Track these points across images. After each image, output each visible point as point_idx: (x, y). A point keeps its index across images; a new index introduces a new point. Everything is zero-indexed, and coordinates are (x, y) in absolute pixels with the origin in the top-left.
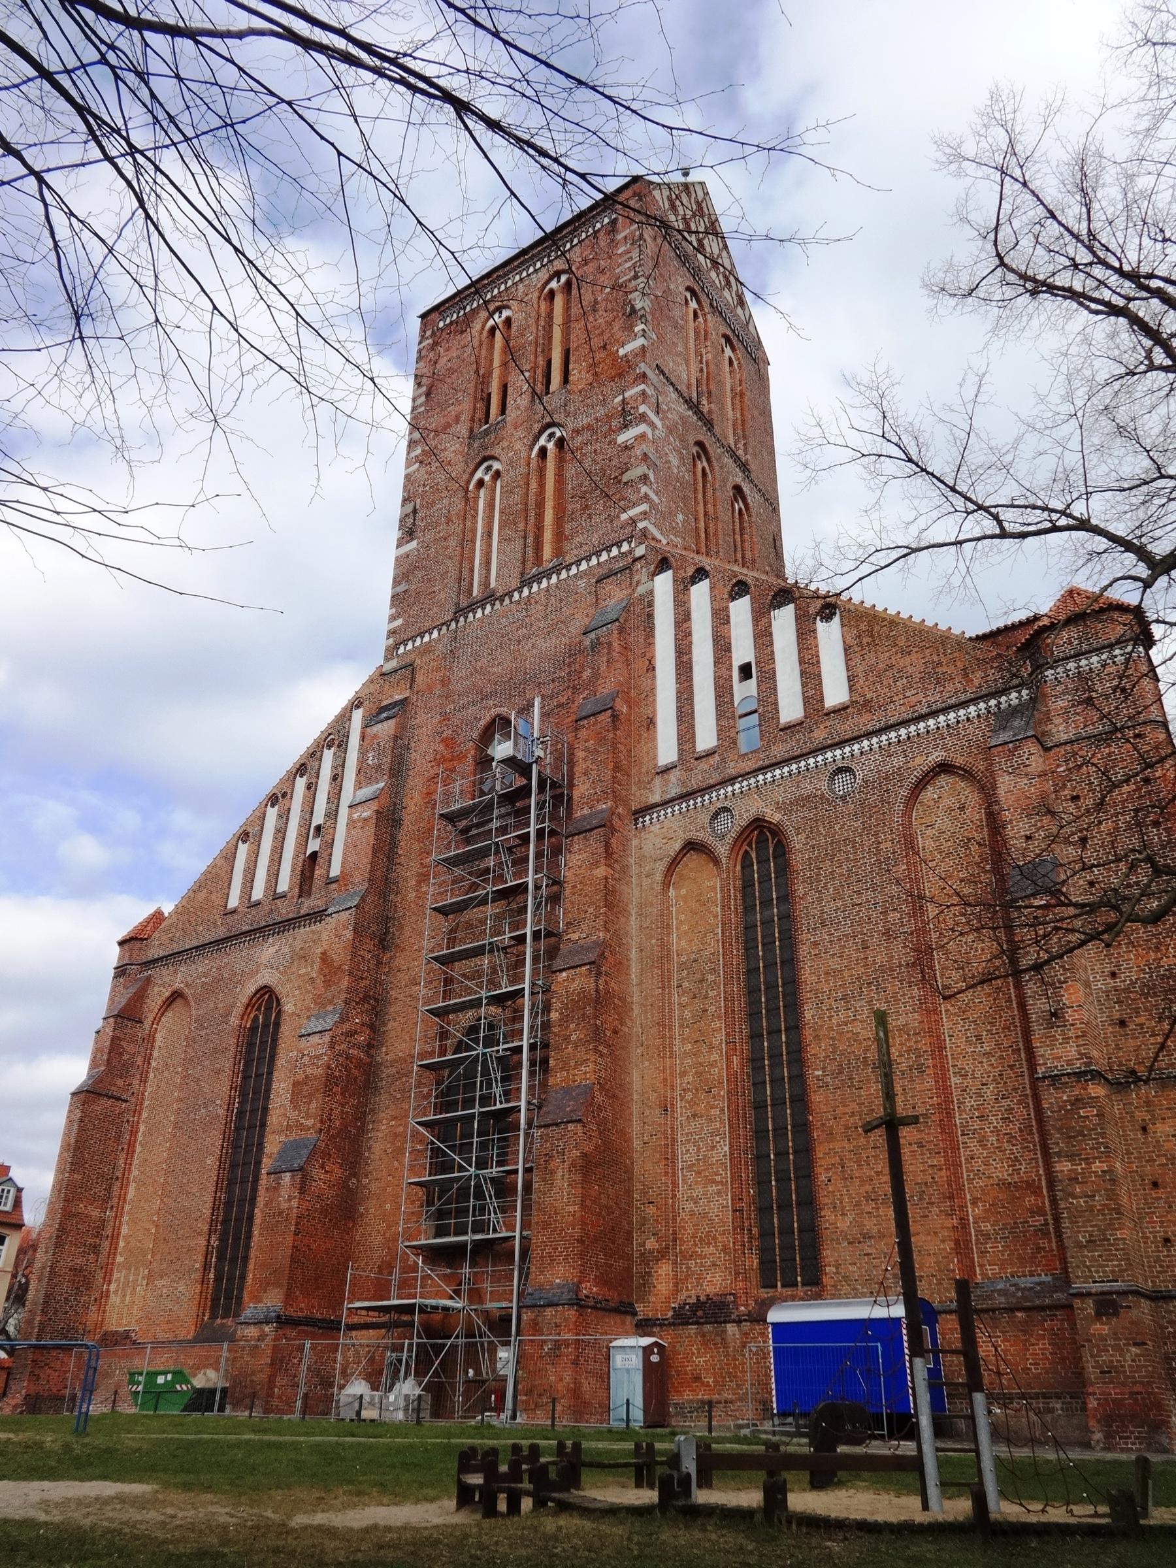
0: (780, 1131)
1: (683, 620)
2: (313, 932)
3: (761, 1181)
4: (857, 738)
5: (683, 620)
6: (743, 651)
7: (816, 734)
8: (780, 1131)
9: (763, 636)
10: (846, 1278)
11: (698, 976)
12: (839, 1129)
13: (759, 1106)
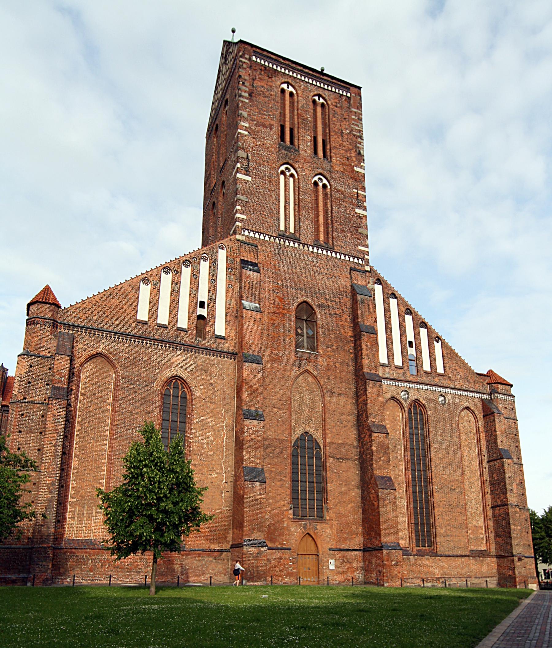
0: (421, 501)
1: (387, 311)
2: (210, 360)
3: (416, 513)
4: (447, 388)
5: (387, 311)
6: (410, 337)
7: (435, 380)
8: (421, 501)
9: (417, 335)
10: (443, 546)
11: (394, 445)
12: (441, 505)
13: (414, 492)
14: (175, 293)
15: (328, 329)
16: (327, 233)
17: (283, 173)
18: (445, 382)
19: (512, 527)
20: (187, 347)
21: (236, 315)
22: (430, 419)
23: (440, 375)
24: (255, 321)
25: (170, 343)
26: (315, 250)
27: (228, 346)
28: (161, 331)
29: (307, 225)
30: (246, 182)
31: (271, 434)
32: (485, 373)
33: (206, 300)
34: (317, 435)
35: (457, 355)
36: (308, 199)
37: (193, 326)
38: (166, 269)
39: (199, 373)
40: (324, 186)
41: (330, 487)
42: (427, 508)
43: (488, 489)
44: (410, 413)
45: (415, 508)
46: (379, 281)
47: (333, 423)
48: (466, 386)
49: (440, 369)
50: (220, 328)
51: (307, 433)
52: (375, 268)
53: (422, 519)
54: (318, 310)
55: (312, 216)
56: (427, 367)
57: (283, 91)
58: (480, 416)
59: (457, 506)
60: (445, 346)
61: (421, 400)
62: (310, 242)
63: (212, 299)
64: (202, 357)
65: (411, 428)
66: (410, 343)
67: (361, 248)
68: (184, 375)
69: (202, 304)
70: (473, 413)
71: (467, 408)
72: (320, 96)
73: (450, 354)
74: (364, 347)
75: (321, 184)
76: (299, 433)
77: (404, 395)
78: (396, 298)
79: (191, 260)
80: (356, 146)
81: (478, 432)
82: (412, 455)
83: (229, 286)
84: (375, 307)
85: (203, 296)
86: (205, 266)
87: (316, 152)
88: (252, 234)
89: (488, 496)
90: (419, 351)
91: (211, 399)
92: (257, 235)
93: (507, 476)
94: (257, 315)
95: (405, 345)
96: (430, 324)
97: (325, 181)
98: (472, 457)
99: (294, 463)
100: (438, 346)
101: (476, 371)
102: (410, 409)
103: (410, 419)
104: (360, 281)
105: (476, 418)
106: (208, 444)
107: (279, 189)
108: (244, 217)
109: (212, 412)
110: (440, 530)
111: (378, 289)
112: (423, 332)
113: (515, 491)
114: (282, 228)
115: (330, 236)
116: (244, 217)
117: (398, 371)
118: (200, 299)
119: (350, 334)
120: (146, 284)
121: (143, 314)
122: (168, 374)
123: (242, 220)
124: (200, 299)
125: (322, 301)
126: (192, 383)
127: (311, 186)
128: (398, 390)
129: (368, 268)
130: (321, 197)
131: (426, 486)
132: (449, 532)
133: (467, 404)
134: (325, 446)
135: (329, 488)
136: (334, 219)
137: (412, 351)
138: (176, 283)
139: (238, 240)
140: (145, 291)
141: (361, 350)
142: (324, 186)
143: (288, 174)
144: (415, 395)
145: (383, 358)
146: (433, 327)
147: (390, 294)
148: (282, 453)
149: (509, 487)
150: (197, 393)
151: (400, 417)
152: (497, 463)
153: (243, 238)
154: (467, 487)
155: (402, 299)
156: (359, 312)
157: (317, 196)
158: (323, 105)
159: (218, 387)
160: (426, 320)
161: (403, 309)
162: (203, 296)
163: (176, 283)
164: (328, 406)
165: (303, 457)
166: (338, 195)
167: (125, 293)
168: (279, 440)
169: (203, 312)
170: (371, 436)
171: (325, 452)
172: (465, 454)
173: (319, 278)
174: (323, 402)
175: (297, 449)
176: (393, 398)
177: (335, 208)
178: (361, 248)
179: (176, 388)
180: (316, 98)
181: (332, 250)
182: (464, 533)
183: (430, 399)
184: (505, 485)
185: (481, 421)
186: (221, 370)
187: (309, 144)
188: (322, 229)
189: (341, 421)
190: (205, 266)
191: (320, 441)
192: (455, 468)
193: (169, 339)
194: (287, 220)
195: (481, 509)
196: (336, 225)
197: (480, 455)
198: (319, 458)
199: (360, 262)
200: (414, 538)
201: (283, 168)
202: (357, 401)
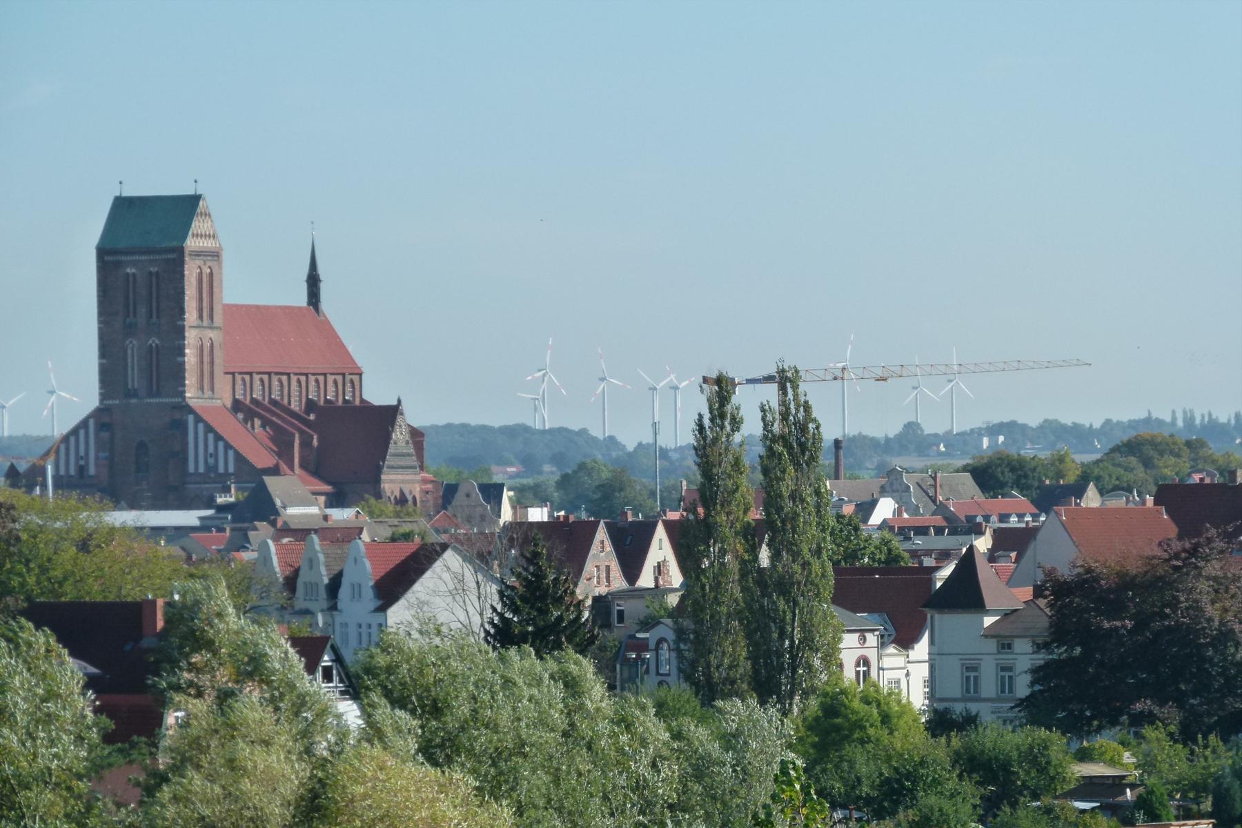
1: (196, 433)
5: (196, 433)
6: (211, 449)
9: (216, 448)
14: (67, 454)
56: (221, 470)
85: (82, 453)
100: (231, 453)
104: (177, 416)
111: (191, 418)
145: (191, 469)
147: (199, 420)
162: (82, 453)
181: (158, 395)
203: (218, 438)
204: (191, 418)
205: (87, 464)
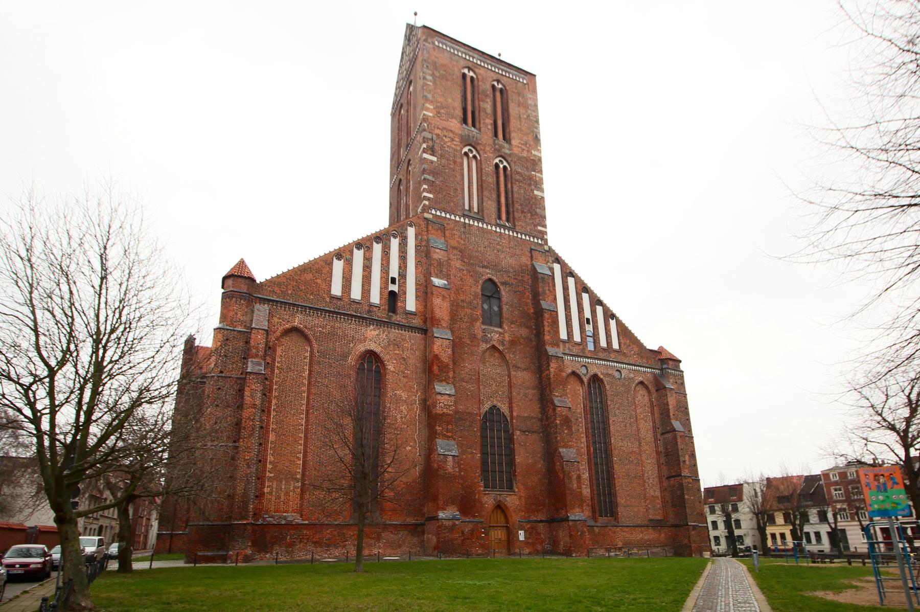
1: (566, 289)
2: (401, 335)
5: (566, 289)
6: (588, 314)
9: (594, 312)
13: (596, 464)
14: (367, 268)
15: (511, 306)
16: (508, 213)
17: (466, 154)
18: (619, 358)
19: (686, 497)
20: (380, 323)
21: (425, 291)
22: (608, 393)
23: (616, 351)
24: (444, 297)
25: (363, 318)
26: (498, 230)
27: (416, 322)
28: (354, 306)
29: (490, 206)
30: (432, 162)
31: (461, 408)
32: (656, 348)
33: (396, 276)
34: (505, 409)
35: (630, 332)
36: (491, 179)
37: (385, 301)
38: (359, 245)
39: (391, 348)
40: (505, 168)
41: (518, 459)
42: (608, 479)
43: (662, 460)
44: (589, 387)
45: (597, 479)
46: (558, 260)
47: (518, 397)
48: (639, 362)
49: (616, 346)
50: (411, 304)
51: (495, 406)
52: (553, 248)
53: (604, 490)
54: (502, 288)
55: (494, 196)
56: (603, 343)
57: (464, 75)
58: (653, 390)
59: (635, 477)
60: (620, 324)
61: (599, 374)
62: (493, 222)
63: (403, 275)
64: (395, 333)
65: (591, 401)
66: (588, 320)
67: (540, 228)
68: (378, 350)
69: (393, 281)
70: (647, 387)
71: (641, 383)
72: (498, 81)
73: (624, 331)
74: (546, 323)
75: (501, 166)
76: (486, 407)
77: (584, 370)
78: (573, 276)
79: (381, 237)
80: (533, 132)
81: (652, 406)
82: (593, 428)
83: (418, 263)
84: (554, 285)
85: (394, 272)
86: (395, 243)
87: (496, 135)
88: (438, 213)
89: (664, 468)
90: (595, 328)
91: (404, 373)
92: (443, 215)
93: (680, 447)
94: (444, 293)
95: (583, 322)
96: (605, 302)
97: (505, 164)
98: (646, 428)
99: (483, 437)
100: (613, 323)
101: (648, 347)
102: (589, 383)
103: (590, 393)
105: (649, 392)
106: (401, 418)
107: (463, 169)
108: (431, 196)
109: (405, 386)
110: (621, 500)
111: (557, 267)
112: (599, 309)
113: (687, 463)
114: (467, 207)
115: (511, 216)
116: (431, 196)
117: (577, 347)
118: (391, 275)
119: (532, 311)
120: (339, 259)
121: (336, 289)
122: (361, 348)
123: (428, 199)
124: (391, 275)
125: (506, 278)
126: (385, 357)
127: (492, 168)
128: (578, 365)
129: (546, 248)
130: (502, 179)
131: (606, 458)
132: (628, 503)
133: (641, 379)
134: (512, 418)
135: (518, 460)
136: (515, 200)
137: (589, 328)
138: (368, 260)
139: (426, 219)
140: (338, 266)
141: (543, 326)
142: (505, 168)
143: (471, 155)
144: (593, 370)
145: (563, 335)
146: (608, 305)
147: (568, 272)
148: (471, 426)
149: (682, 459)
150: (390, 367)
151: (581, 391)
152: (669, 436)
153: (430, 216)
154: (643, 458)
155: (579, 278)
156: (541, 290)
157: (498, 178)
158: (501, 90)
159: (411, 362)
160: (602, 299)
161: (580, 288)
162: (394, 272)
163: (368, 260)
164: (514, 380)
165: (492, 430)
166: (518, 177)
167: (319, 268)
168: (469, 413)
169: (395, 288)
170: (554, 410)
171: (512, 425)
172: (641, 426)
173: (502, 256)
174: (509, 376)
175: (486, 423)
176: (574, 373)
177: (515, 189)
178: (540, 228)
179: (370, 362)
180: (495, 83)
181: (513, 229)
182: (643, 504)
183: (607, 374)
184: (678, 457)
185: (654, 395)
186: (412, 344)
187: (490, 127)
188: (503, 209)
189: (526, 395)
190: (395, 243)
191: (507, 413)
192: (632, 440)
193: (362, 315)
194: (470, 198)
195: (657, 480)
196: (517, 206)
197: (654, 427)
198: (506, 431)
199: (540, 242)
200: (597, 508)
201: (466, 149)
202: (540, 376)
203: (596, 301)
204: (557, 267)
205: (403, 285)
